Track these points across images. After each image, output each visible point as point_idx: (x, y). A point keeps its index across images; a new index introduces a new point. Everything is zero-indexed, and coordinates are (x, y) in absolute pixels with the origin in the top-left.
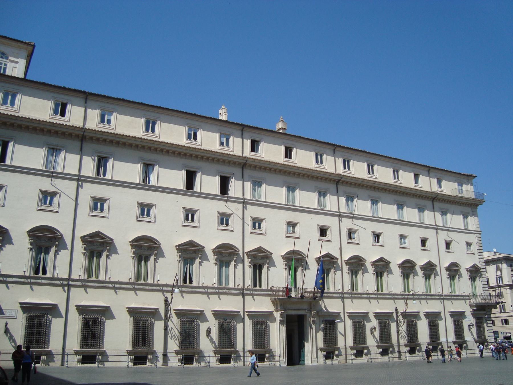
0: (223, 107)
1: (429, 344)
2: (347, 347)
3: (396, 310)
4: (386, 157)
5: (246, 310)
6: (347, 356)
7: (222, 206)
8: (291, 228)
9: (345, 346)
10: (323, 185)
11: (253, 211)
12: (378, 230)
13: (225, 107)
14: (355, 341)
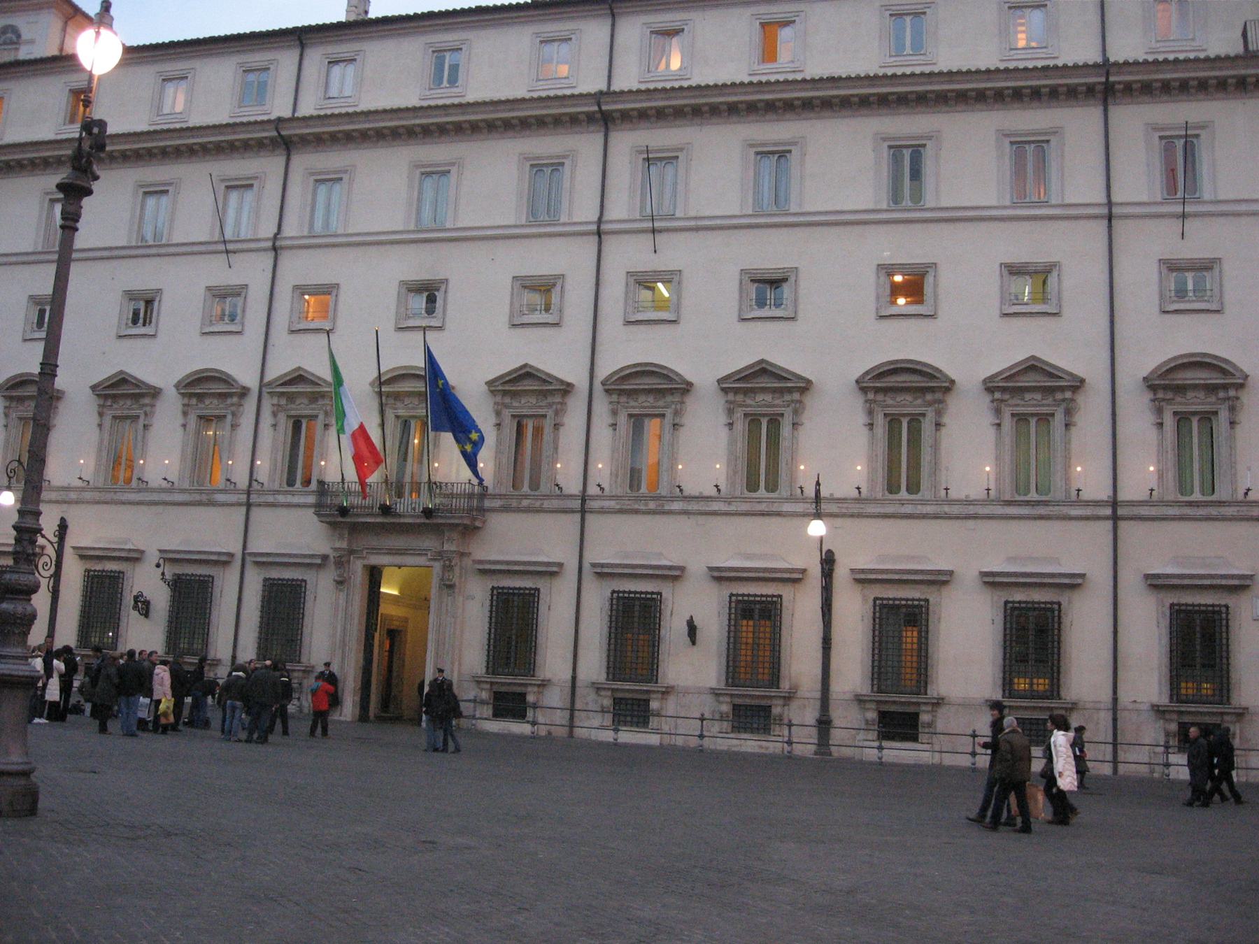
2: (579, 684)
3: (828, 561)
6: (577, 713)
7: (217, 272)
9: (574, 678)
14: (617, 665)
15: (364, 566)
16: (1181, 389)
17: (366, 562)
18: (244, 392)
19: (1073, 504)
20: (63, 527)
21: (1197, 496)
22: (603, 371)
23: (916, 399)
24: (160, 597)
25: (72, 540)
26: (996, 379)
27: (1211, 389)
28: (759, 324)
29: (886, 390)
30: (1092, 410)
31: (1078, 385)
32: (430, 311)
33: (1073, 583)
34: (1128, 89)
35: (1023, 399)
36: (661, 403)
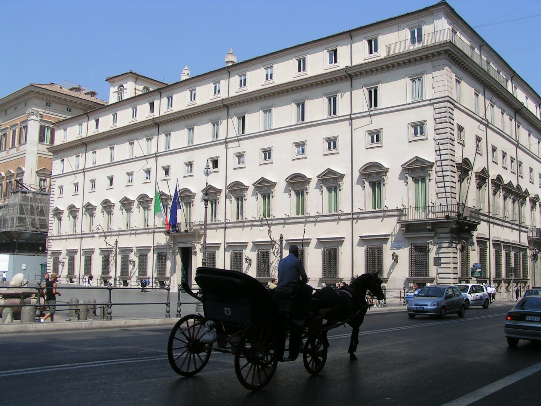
0: (186, 68)
1: (321, 281)
3: (281, 238)
4: (285, 50)
5: (82, 248)
8: (190, 167)
10: (214, 116)
11: (163, 161)
12: (266, 146)
13: (188, 68)
15: (178, 248)
16: (369, 175)
17: (178, 246)
18: (152, 199)
19: (341, 215)
20: (117, 242)
21: (377, 209)
22: (228, 184)
23: (301, 185)
24: (136, 260)
25: (118, 246)
26: (320, 177)
27: (378, 173)
28: (265, 166)
29: (294, 183)
30: (346, 184)
31: (342, 176)
32: (191, 171)
33: (340, 241)
34: (356, 75)
35: (328, 182)
36: (241, 193)
